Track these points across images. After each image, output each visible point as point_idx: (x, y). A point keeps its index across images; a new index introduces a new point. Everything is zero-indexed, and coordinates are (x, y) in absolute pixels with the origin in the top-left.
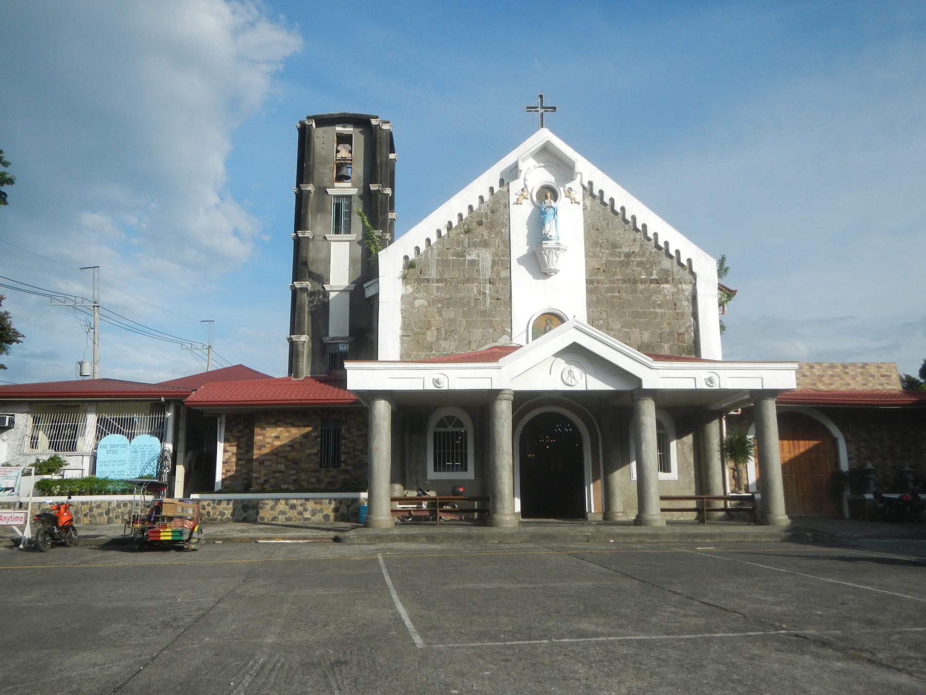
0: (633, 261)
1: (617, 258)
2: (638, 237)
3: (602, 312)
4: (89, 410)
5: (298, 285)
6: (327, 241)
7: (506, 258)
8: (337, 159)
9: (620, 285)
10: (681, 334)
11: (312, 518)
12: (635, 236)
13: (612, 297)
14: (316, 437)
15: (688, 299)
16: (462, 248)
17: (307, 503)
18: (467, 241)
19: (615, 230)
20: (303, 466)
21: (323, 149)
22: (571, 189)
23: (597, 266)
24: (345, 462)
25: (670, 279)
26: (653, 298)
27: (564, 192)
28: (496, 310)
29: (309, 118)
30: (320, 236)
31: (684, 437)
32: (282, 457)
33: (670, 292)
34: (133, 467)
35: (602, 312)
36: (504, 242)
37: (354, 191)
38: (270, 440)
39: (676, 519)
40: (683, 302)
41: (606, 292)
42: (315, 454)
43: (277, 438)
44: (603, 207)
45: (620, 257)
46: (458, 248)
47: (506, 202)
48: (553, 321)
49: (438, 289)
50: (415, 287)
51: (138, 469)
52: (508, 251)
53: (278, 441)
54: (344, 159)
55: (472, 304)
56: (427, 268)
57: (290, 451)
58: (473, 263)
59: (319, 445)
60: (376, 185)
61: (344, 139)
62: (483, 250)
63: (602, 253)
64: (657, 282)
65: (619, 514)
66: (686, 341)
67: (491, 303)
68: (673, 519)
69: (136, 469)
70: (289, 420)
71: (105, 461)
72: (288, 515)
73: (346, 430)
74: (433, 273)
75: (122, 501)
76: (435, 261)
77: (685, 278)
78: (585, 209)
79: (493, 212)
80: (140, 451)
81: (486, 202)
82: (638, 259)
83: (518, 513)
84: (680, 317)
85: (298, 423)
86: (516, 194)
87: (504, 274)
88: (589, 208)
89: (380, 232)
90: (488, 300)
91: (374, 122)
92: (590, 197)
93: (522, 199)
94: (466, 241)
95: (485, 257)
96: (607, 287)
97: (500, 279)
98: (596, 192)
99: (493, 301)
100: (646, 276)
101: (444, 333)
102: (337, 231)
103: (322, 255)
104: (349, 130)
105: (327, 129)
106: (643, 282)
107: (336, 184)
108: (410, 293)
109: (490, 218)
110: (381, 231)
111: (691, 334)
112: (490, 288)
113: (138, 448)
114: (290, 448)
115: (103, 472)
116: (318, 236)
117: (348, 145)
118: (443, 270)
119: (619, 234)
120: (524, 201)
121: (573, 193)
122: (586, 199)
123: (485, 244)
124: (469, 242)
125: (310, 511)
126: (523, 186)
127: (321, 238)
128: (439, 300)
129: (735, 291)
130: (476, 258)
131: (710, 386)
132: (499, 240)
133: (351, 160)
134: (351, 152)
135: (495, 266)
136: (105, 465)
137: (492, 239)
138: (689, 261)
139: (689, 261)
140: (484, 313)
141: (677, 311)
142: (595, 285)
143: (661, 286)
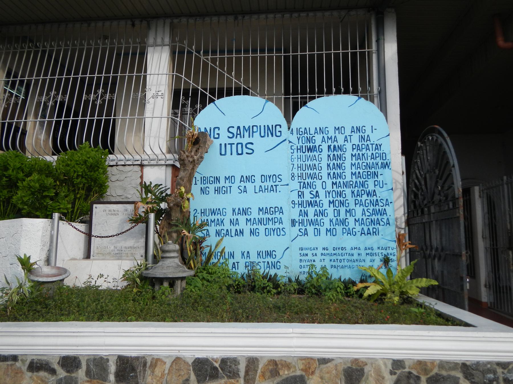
4: (151, 41)
34: (307, 197)
51: (326, 202)
69: (316, 204)
71: (217, 179)
75: (421, 364)
80: (325, 147)
113: (318, 138)
115: (213, 212)
136: (217, 191)
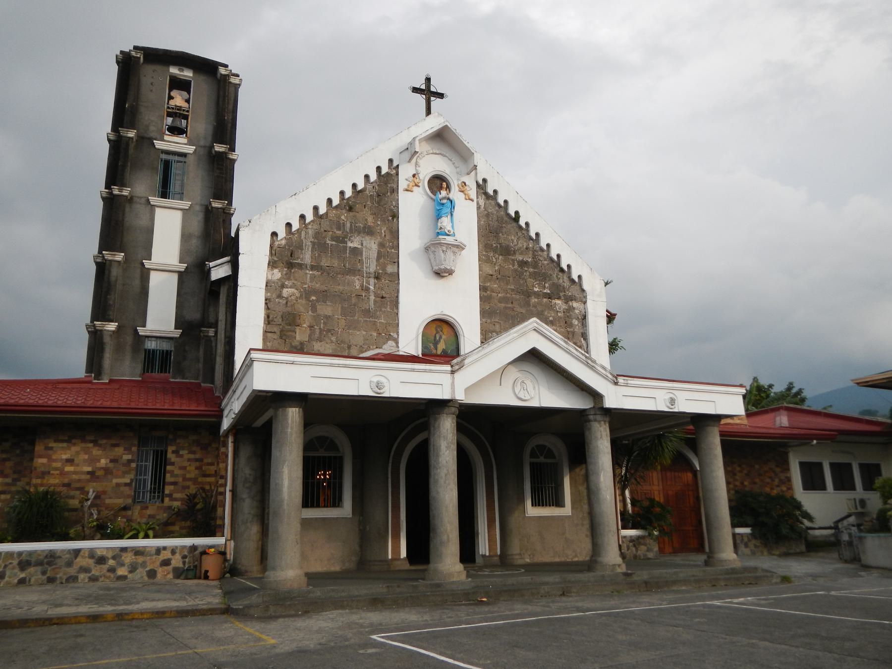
1: (511, 266)
2: (530, 246)
3: (496, 324)
5: (108, 255)
6: (149, 206)
7: (393, 250)
8: (170, 106)
9: (513, 295)
11: (130, 576)
12: (529, 245)
13: (506, 308)
14: (130, 461)
15: (578, 318)
16: (343, 233)
17: (124, 555)
18: (349, 226)
19: (508, 235)
20: (108, 501)
21: (151, 91)
23: (491, 273)
24: (170, 496)
25: (561, 294)
27: (458, 186)
28: (381, 310)
29: (136, 48)
30: (141, 198)
32: (77, 489)
33: (562, 309)
35: (496, 324)
36: (391, 232)
37: (190, 149)
38: (59, 465)
39: (570, 560)
40: (574, 320)
41: (500, 302)
42: (126, 485)
43: (70, 461)
44: (497, 208)
45: (513, 265)
46: (338, 232)
47: (395, 186)
48: (444, 329)
49: (313, 278)
50: (284, 272)
52: (395, 243)
53: (71, 465)
54: (180, 108)
55: (354, 300)
56: (300, 251)
57: (88, 481)
58: (356, 252)
59: (134, 472)
60: (223, 145)
61: (178, 84)
62: (368, 238)
63: (496, 259)
64: (549, 297)
65: (517, 557)
67: (375, 301)
68: (568, 560)
70: (92, 438)
72: (93, 572)
73: (173, 452)
74: (307, 257)
76: (310, 243)
78: (479, 208)
79: (380, 195)
81: (372, 183)
82: (531, 270)
83: (404, 559)
85: (104, 442)
86: (407, 180)
87: (390, 269)
89: (225, 203)
90: (372, 298)
93: (413, 186)
94: (348, 225)
95: (370, 247)
96: (500, 297)
97: (386, 273)
98: (490, 191)
99: (378, 299)
100: (539, 288)
101: (317, 331)
102: (164, 195)
103: (143, 222)
104: (188, 74)
105: (159, 68)
106: (537, 295)
107: (166, 138)
108: (278, 280)
109: (375, 202)
110: (226, 202)
112: (375, 284)
114: (88, 477)
116: (138, 197)
117: (186, 93)
118: (319, 255)
119: (512, 240)
120: (415, 189)
122: (480, 197)
123: (369, 231)
124: (351, 225)
125: (128, 566)
126: (414, 172)
127: (143, 201)
128: (314, 292)
129: (615, 315)
130: (360, 247)
132: (385, 228)
133: (188, 111)
134: (188, 101)
135: (381, 259)
137: (377, 226)
138: (580, 277)
139: (580, 277)
140: (367, 312)
142: (488, 292)
143: (553, 301)
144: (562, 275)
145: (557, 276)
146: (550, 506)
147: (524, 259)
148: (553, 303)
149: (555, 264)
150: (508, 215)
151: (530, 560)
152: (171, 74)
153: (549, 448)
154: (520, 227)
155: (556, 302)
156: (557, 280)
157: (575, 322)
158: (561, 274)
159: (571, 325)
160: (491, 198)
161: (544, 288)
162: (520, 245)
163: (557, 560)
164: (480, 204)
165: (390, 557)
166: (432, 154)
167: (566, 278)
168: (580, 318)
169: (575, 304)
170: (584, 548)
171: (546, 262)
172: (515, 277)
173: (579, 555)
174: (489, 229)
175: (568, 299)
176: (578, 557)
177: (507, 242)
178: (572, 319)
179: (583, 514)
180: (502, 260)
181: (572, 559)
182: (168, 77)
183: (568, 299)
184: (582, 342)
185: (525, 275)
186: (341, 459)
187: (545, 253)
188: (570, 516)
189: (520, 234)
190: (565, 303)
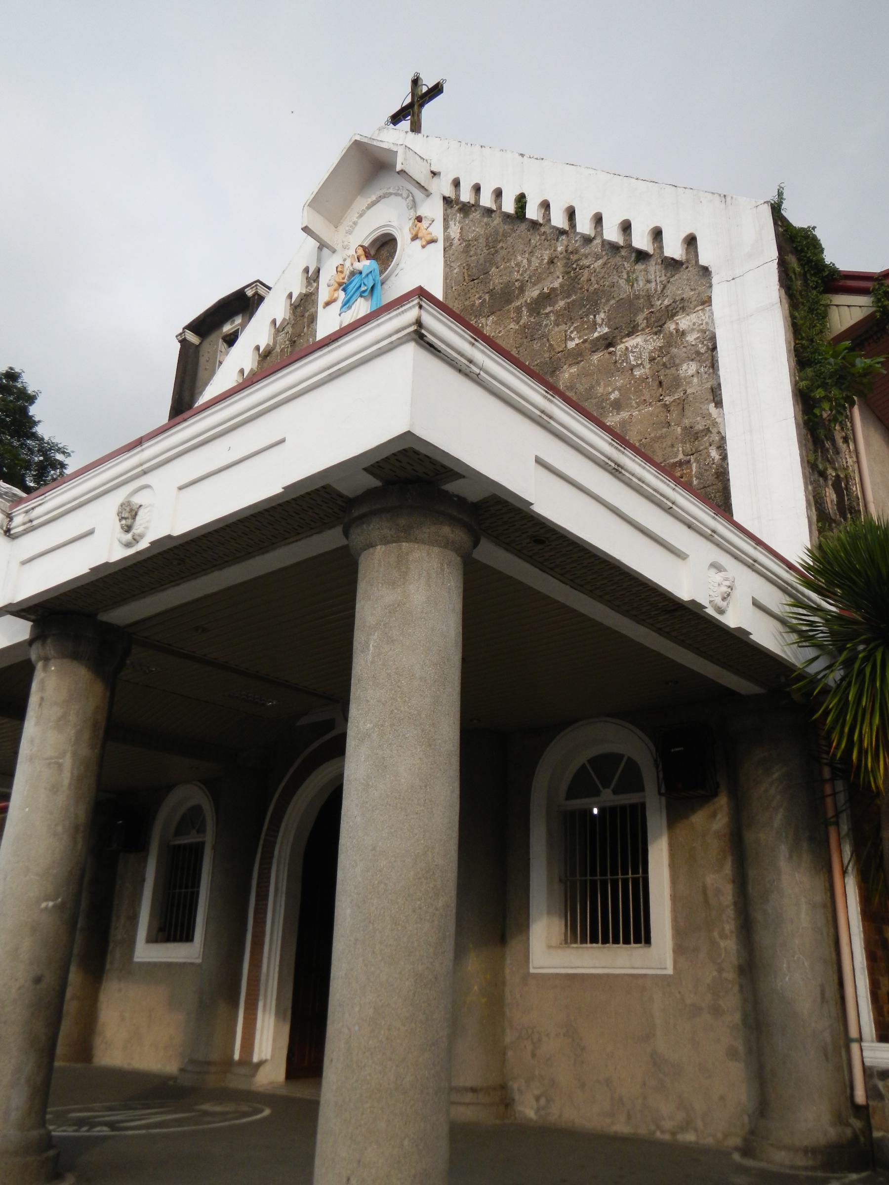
0: (549, 313)
1: (512, 326)
2: (559, 249)
10: (680, 464)
12: (555, 251)
15: (698, 353)
19: (509, 260)
22: (419, 219)
25: (640, 319)
26: (600, 390)
29: (184, 329)
31: (693, 810)
33: (646, 356)
39: (667, 1137)
40: (685, 367)
44: (485, 220)
47: (313, 310)
64: (608, 342)
66: (695, 482)
68: (658, 1134)
77: (685, 296)
79: (295, 342)
82: (561, 304)
84: (674, 416)
88: (456, 242)
91: (249, 293)
92: (458, 215)
100: (579, 338)
106: (577, 356)
111: (709, 456)
121: (425, 224)
122: (452, 223)
131: (128, 545)
138: (691, 241)
139: (691, 241)
141: (668, 399)
144: (643, 267)
145: (628, 280)
146: (627, 941)
147: (546, 290)
148: (618, 353)
149: (623, 253)
150: (507, 216)
151: (536, 1113)
152: (223, 335)
153: (629, 758)
154: (535, 224)
155: (627, 344)
156: (627, 288)
157: (689, 368)
158: (640, 267)
159: (677, 383)
160: (473, 209)
161: (594, 326)
162: (535, 262)
163: (621, 1127)
164: (453, 235)
165: (237, 1056)
166: (369, 207)
167: (654, 269)
168: (703, 350)
169: (684, 322)
170: (722, 1098)
171: (600, 262)
172: (521, 345)
173: (700, 1124)
174: (469, 276)
175: (657, 325)
176: (696, 1130)
177: (505, 279)
178: (677, 366)
179: (720, 970)
180: (493, 323)
181: (673, 1134)
182: (221, 340)
183: (657, 325)
184: (710, 414)
185: (546, 325)
186: (203, 844)
187: (598, 241)
188: (670, 976)
189: (535, 239)
190: (656, 334)
